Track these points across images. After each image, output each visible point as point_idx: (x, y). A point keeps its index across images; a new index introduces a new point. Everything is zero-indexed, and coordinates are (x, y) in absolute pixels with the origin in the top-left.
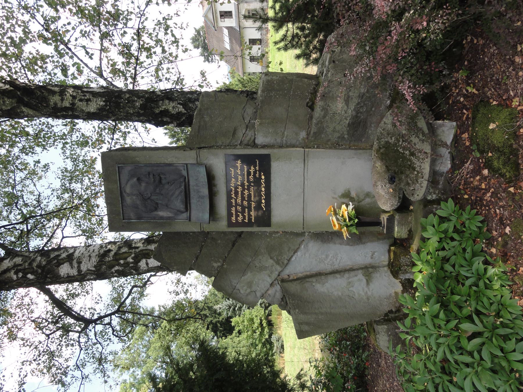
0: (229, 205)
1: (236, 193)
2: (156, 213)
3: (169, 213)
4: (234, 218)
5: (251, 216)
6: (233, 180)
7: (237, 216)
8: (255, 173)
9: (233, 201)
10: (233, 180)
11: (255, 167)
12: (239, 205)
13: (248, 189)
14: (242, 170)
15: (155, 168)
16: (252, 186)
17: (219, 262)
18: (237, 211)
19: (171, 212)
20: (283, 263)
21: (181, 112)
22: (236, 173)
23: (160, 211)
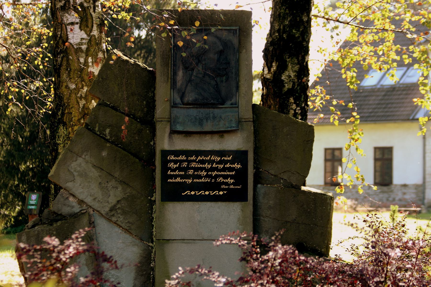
0: (188, 153)
1: (202, 162)
2: (181, 67)
3: (180, 82)
4: (173, 158)
5: (175, 179)
6: (219, 159)
7: (175, 162)
8: (227, 184)
9: (193, 158)
10: (219, 159)
11: (233, 184)
12: (188, 165)
13: (207, 176)
14: (230, 169)
15: (234, 71)
16: (211, 180)
17: (111, 137)
18: (181, 161)
19: (182, 85)
20: (113, 215)
21: (284, 86)
22: (226, 162)
23: (183, 73)
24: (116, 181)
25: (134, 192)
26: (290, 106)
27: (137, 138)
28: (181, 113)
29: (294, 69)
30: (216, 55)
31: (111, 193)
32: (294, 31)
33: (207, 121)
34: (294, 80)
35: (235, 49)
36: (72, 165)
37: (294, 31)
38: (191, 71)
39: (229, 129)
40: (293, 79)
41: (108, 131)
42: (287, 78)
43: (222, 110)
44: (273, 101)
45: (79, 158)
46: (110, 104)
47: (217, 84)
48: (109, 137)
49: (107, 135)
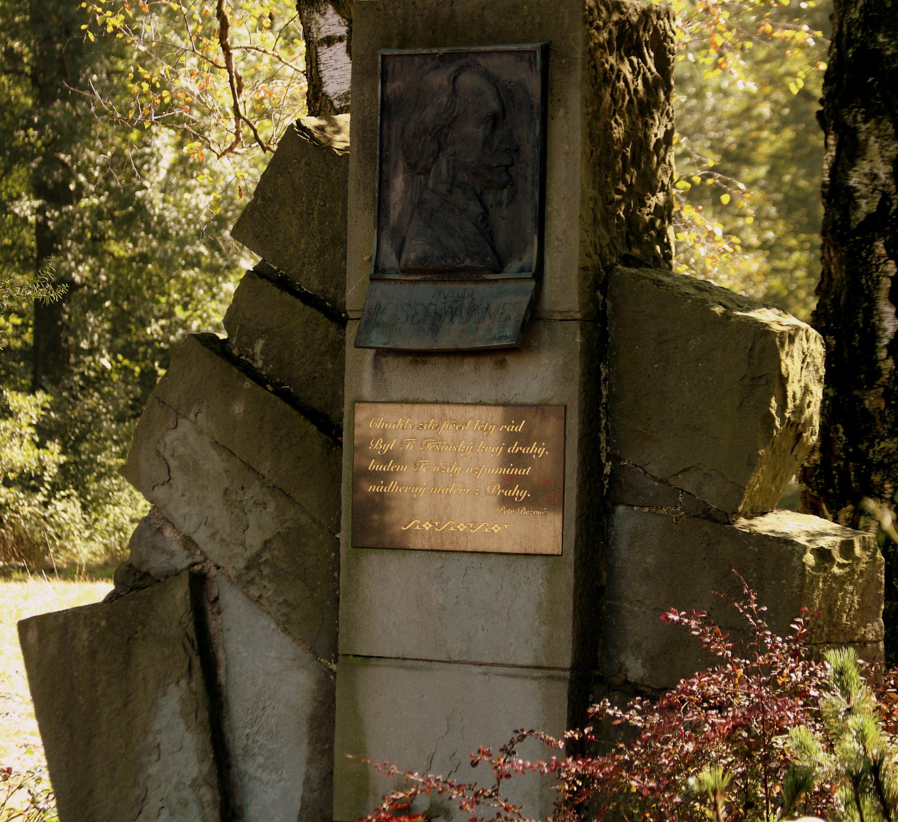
2: (401, 164)
3: (398, 208)
17: (266, 364)
19: (401, 215)
20: (252, 582)
21: (857, 207)
23: (405, 181)
24: (263, 485)
25: (304, 519)
26: (877, 266)
27: (330, 366)
28: (397, 295)
29: (887, 154)
30: (482, 127)
31: (252, 519)
32: (881, 39)
33: (452, 320)
34: (889, 186)
35: (532, 107)
36: (167, 439)
37: (881, 39)
38: (424, 174)
39: (496, 344)
40: (884, 186)
41: (259, 346)
42: (866, 181)
43: (496, 285)
44: (834, 252)
45: (181, 421)
46: (279, 270)
47: (486, 211)
48: (260, 364)
49: (258, 357)
